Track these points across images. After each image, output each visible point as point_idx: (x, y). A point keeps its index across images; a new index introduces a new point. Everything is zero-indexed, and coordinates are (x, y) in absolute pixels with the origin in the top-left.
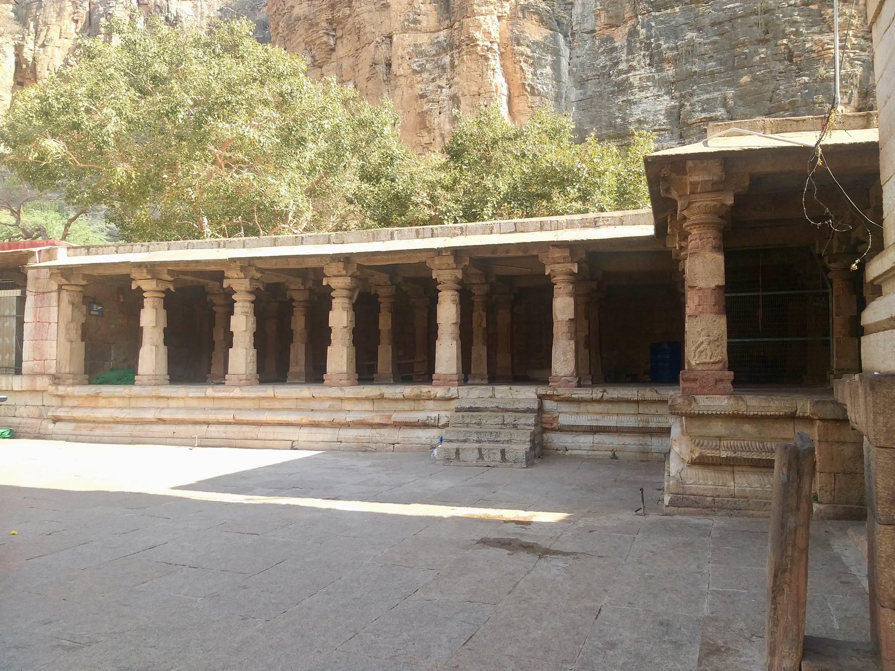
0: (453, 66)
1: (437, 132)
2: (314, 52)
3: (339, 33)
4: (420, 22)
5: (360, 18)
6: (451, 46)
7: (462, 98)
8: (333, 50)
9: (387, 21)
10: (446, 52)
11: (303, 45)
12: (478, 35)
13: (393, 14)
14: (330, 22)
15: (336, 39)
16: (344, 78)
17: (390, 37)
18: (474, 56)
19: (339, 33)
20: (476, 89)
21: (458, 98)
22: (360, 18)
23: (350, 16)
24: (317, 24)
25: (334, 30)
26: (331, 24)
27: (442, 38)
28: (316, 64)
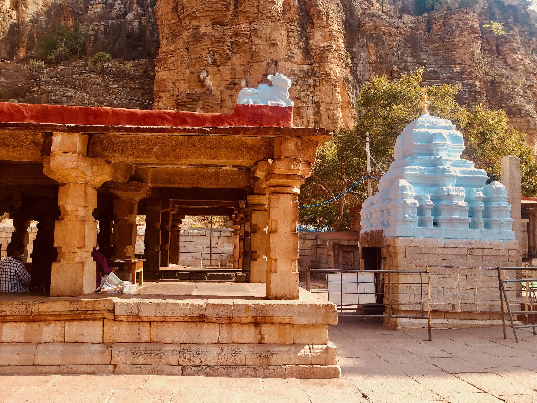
0: (315, 85)
1: (305, 119)
2: (215, 57)
3: (236, 50)
4: (294, 58)
5: (258, 46)
6: (313, 74)
7: (321, 104)
8: (230, 59)
9: (275, 53)
10: (310, 77)
11: (207, 51)
12: (332, 73)
13: (279, 50)
14: (232, 43)
15: (233, 53)
16: (236, 76)
18: (329, 83)
19: (236, 50)
20: (329, 101)
21: (319, 103)
22: (258, 46)
23: (247, 43)
25: (232, 48)
26: (231, 44)
27: (305, 69)
28: (216, 64)
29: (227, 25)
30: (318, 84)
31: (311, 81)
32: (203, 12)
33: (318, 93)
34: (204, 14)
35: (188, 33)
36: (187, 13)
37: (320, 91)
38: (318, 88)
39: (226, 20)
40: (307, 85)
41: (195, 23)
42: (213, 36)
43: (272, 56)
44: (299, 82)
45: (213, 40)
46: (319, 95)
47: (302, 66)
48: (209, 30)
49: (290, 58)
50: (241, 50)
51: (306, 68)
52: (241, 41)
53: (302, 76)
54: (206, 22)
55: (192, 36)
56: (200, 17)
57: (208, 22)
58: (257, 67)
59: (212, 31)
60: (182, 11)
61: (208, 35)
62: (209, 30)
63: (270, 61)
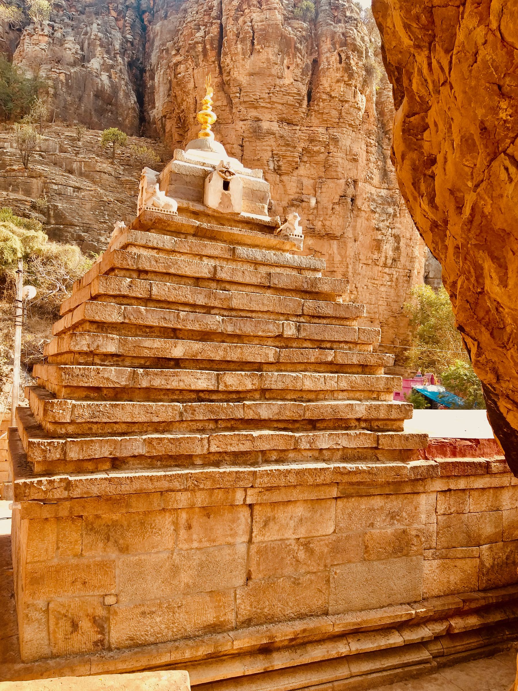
17: (355, 182)
24: (295, 147)
29: (297, 125)
30: (398, 215)
31: (391, 210)
32: (269, 103)
33: (398, 225)
34: (269, 106)
35: (244, 125)
36: (246, 99)
37: (401, 223)
38: (398, 220)
39: (296, 119)
40: (387, 214)
41: (253, 113)
42: (282, 137)
43: (351, 175)
44: (377, 209)
45: (281, 142)
46: (399, 228)
47: (378, 190)
48: (275, 127)
49: (368, 180)
50: (312, 159)
51: (384, 192)
52: (315, 149)
53: (380, 202)
54: (270, 116)
55: (251, 130)
56: (263, 107)
57: (275, 117)
58: (333, 184)
59: (278, 129)
60: (238, 95)
61: (274, 134)
62: (275, 127)
63: (349, 180)
